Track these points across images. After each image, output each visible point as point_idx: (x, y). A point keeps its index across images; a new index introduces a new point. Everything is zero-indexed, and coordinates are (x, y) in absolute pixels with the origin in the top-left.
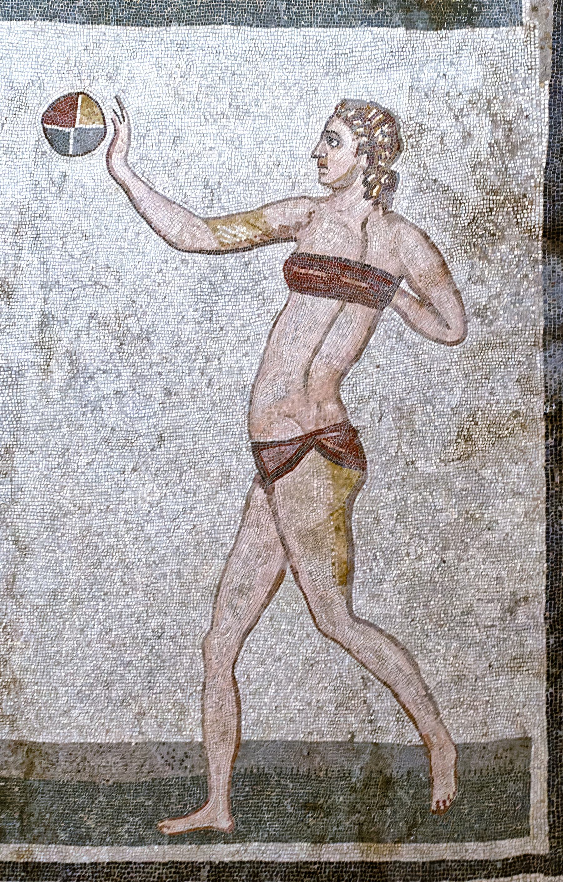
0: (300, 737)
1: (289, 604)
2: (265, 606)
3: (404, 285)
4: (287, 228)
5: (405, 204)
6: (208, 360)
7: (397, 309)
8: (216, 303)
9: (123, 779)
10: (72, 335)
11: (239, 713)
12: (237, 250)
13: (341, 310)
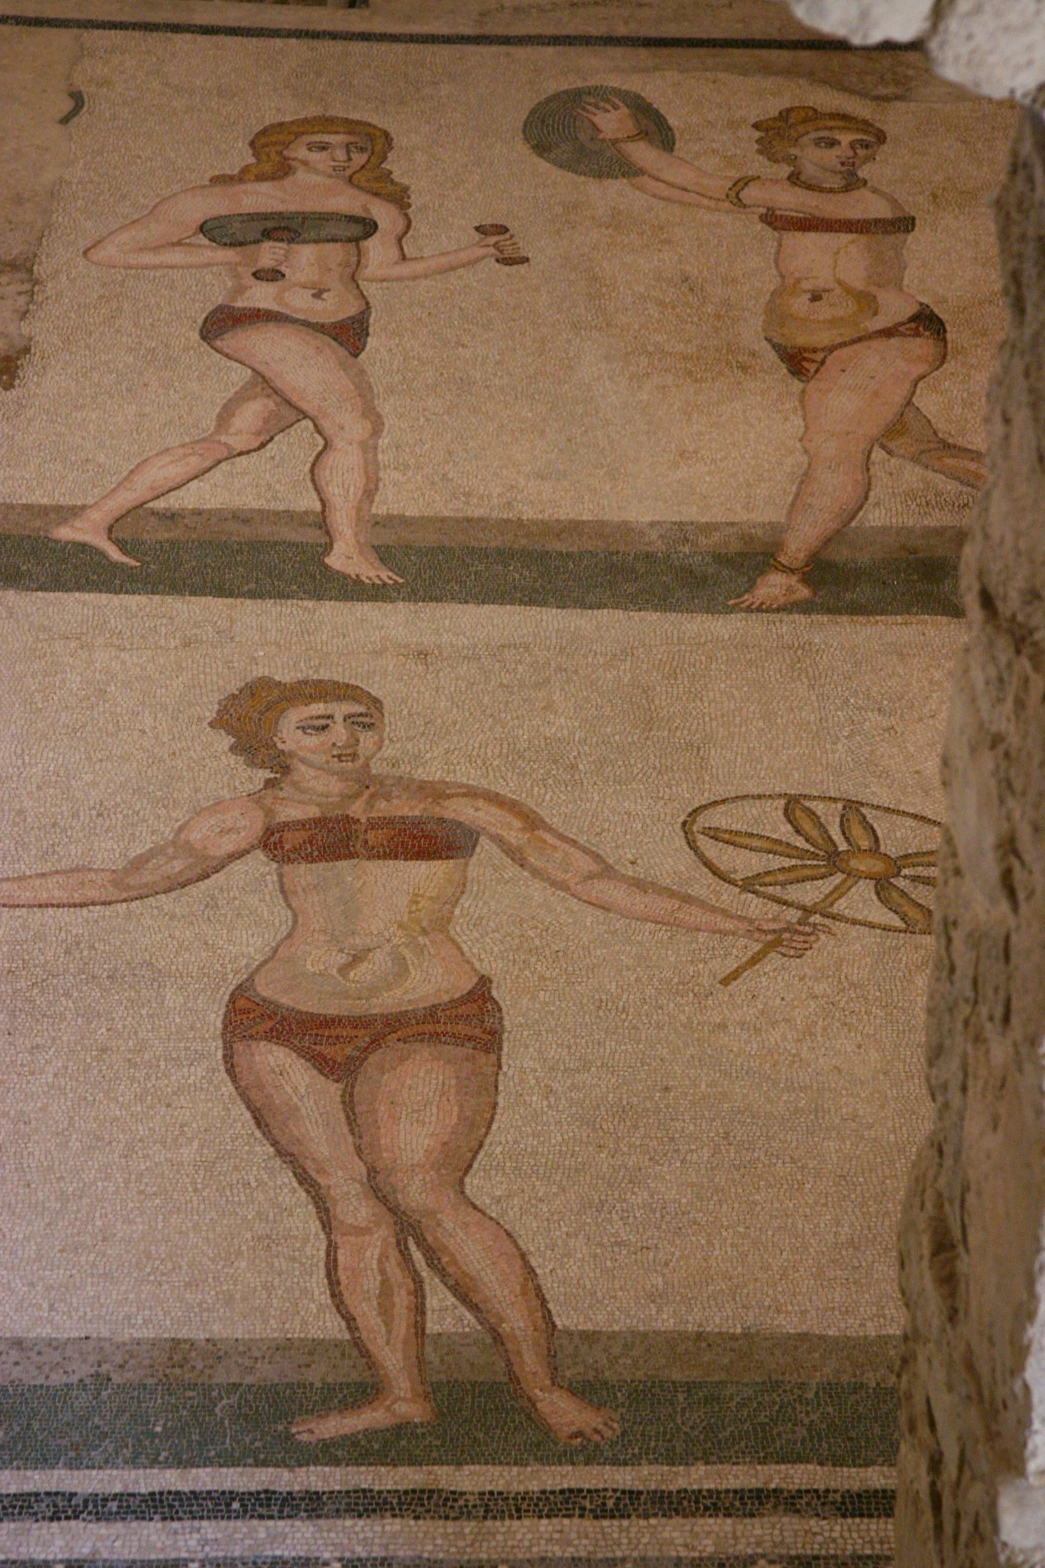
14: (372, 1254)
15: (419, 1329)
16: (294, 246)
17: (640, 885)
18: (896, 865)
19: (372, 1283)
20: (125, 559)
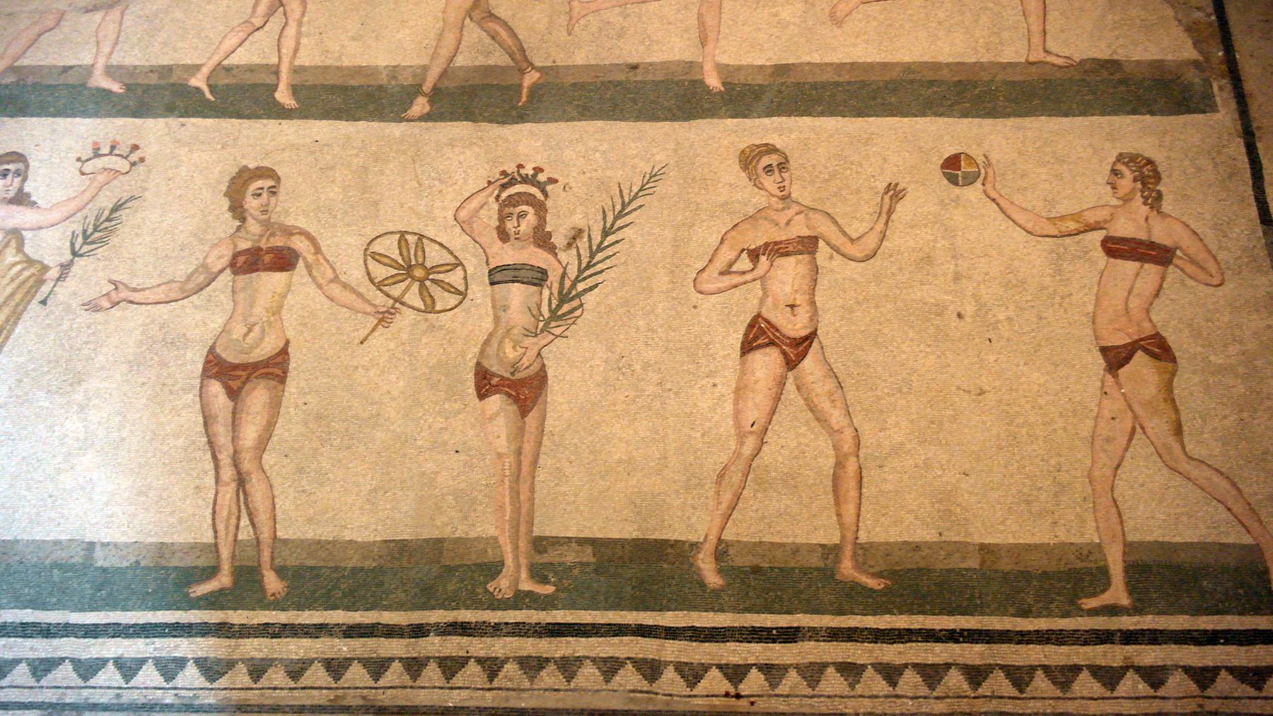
0: (1167, 539)
1: (1142, 448)
2: (1126, 450)
3: (1178, 253)
6: (1062, 298)
7: (1177, 266)
8: (1061, 265)
9: (1048, 569)
10: (975, 284)
11: (1122, 522)
12: (1070, 235)
13: (1142, 267)
14: (228, 496)
15: (236, 535)
17: (345, 286)
18: (429, 271)
19: (225, 513)
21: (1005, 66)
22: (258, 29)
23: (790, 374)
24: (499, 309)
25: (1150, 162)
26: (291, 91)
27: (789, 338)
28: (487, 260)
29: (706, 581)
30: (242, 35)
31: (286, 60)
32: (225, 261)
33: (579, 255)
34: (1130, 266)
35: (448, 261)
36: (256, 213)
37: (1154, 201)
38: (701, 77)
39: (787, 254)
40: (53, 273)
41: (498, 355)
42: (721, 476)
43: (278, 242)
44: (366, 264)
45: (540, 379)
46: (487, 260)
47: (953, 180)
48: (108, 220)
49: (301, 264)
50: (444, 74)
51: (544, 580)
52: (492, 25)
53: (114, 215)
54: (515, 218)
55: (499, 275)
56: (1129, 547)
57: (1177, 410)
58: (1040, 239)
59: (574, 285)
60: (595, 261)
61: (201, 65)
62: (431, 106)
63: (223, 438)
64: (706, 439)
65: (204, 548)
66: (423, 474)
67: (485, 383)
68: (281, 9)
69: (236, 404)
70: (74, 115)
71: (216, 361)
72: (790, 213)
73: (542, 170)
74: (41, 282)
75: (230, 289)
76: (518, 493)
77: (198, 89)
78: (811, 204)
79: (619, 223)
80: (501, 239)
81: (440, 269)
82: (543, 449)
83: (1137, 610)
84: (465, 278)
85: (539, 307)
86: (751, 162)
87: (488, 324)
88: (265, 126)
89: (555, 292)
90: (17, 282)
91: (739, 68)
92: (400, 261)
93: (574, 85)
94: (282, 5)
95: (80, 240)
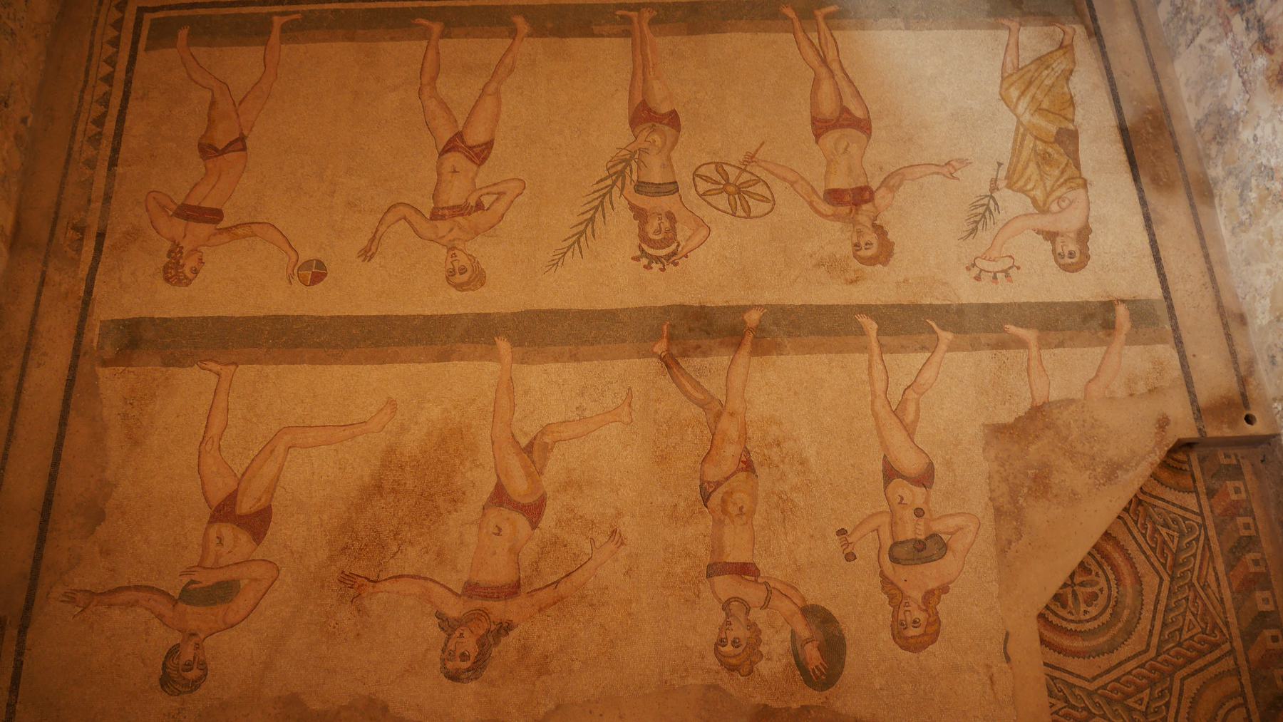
0: (240, 48)
2: (249, 92)
3: (171, 213)
4: (220, 234)
5: (166, 245)
7: (175, 204)
13: (200, 203)
14: (830, 53)
16: (914, 537)
17: (784, 179)
18: (724, 190)
19: (829, 45)
20: (930, 322)
21: (257, 361)
22: (909, 387)
23: (460, 129)
24: (668, 165)
25: (167, 280)
26: (865, 329)
27: (459, 151)
28: (681, 199)
29: (523, 19)
30: (921, 380)
31: (876, 358)
32: (878, 196)
33: (611, 203)
34: (207, 204)
35: (710, 197)
36: (866, 230)
37: (175, 251)
38: (514, 349)
39: (454, 207)
40: (1002, 184)
41: (665, 137)
42: (511, 71)
43: (844, 210)
44: (772, 194)
45: (635, 121)
46: (681, 199)
47: (320, 264)
48: (977, 222)
49: (821, 195)
50: (739, 345)
51: (622, 17)
52: (699, 396)
53: (974, 225)
54: (663, 230)
55: (672, 188)
56: (265, 44)
57: (209, 116)
58: (266, 221)
59: (614, 183)
60: (599, 200)
61: (947, 351)
62: (743, 320)
63: (843, 84)
64: (520, 91)
65: (838, 28)
66: (706, 68)
67: (673, 119)
68: (894, 408)
69: (841, 104)
70: (1038, 304)
71: (865, 129)
72: (450, 237)
73: (645, 267)
74: (1008, 177)
75: (868, 176)
76: (643, 59)
77: (943, 329)
78: (432, 244)
79: (582, 228)
80: (672, 214)
81: (714, 192)
82: (629, 82)
83: (271, 14)
84: (696, 186)
85: (639, 167)
86: (477, 276)
87: (675, 155)
88: (878, 299)
89: (627, 177)
90: (1025, 177)
91: (481, 358)
92: (745, 196)
93: (624, 341)
94: (894, 412)
95: (992, 208)
